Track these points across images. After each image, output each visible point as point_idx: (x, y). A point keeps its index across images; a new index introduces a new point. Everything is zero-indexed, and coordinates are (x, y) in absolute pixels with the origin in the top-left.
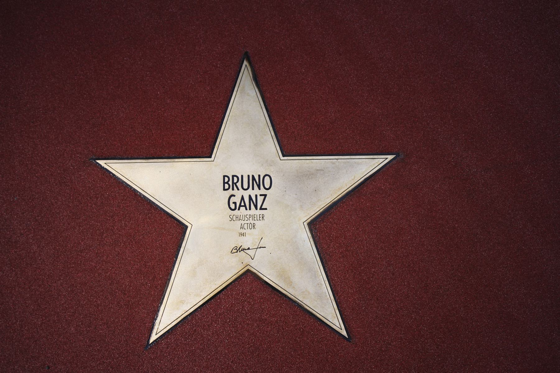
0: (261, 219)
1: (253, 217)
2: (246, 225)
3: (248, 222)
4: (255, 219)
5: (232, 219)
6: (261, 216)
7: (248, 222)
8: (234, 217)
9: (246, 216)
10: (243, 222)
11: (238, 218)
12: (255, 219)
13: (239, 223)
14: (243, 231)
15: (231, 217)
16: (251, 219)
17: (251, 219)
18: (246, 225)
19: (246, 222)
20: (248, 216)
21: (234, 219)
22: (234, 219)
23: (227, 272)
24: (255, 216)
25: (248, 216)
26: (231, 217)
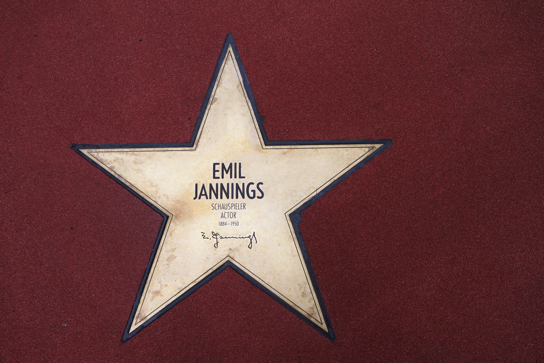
0: (242, 207)
2: (226, 214)
4: (237, 208)
5: (214, 208)
6: (242, 205)
9: (228, 205)
10: (223, 211)
12: (237, 208)
14: (223, 220)
16: (233, 207)
17: (233, 207)
18: (226, 214)
20: (230, 205)
21: (217, 207)
22: (217, 207)
24: (237, 205)
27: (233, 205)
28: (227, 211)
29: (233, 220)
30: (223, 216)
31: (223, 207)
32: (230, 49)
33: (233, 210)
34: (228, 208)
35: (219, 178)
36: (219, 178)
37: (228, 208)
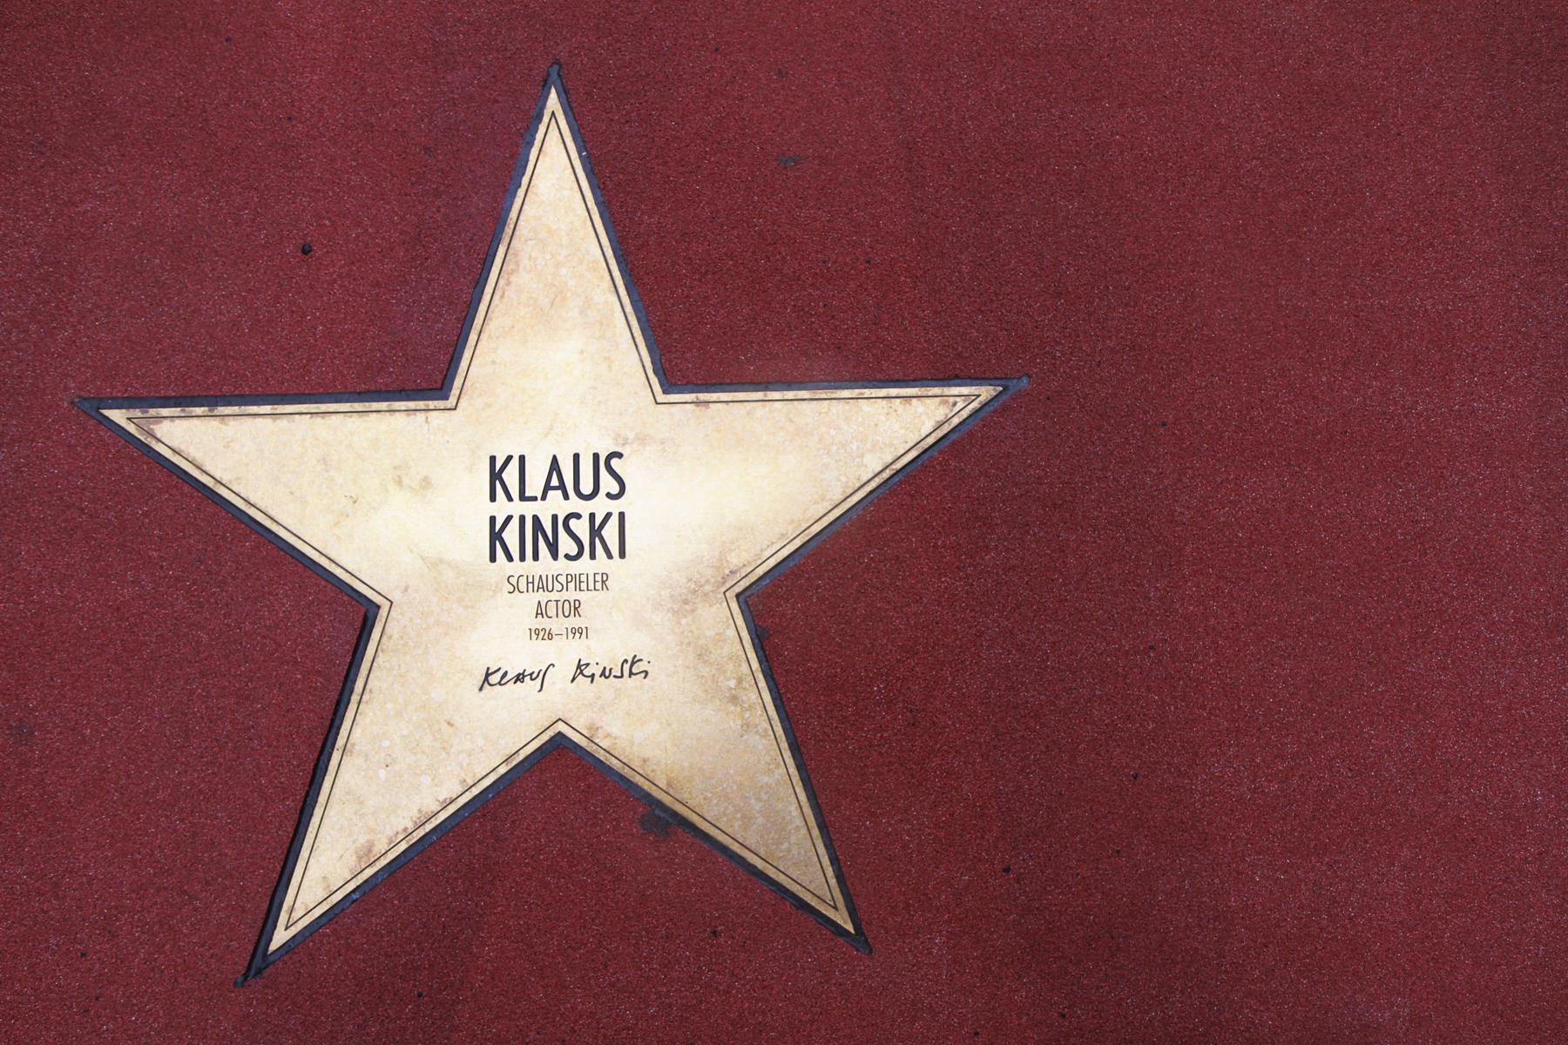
0: (599, 585)
1: (576, 580)
3: (564, 595)
4: (584, 586)
5: (516, 588)
6: (598, 578)
7: (564, 595)
8: (523, 581)
9: (556, 578)
10: (543, 596)
12: (584, 586)
13: (532, 599)
14: (542, 623)
16: (571, 585)
17: (571, 585)
18: (552, 605)
19: (554, 596)
20: (562, 579)
21: (523, 586)
22: (523, 586)
24: (583, 578)
27: (571, 578)
28: (554, 596)
29: (574, 622)
30: (541, 612)
31: (541, 585)
32: (553, 102)
33: (572, 595)
35: (535, 499)
36: (535, 499)
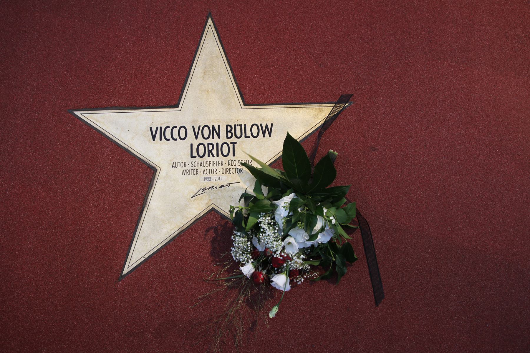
0: (220, 165)
1: (213, 163)
3: (208, 168)
4: (215, 165)
6: (220, 162)
7: (208, 168)
11: (201, 165)
12: (215, 165)
15: (193, 163)
16: (211, 165)
20: (208, 163)
21: (196, 165)
22: (196, 165)
23: (196, 209)
25: (208, 163)
26: (193, 163)
33: (211, 167)
34: (207, 165)
37: (207, 165)
